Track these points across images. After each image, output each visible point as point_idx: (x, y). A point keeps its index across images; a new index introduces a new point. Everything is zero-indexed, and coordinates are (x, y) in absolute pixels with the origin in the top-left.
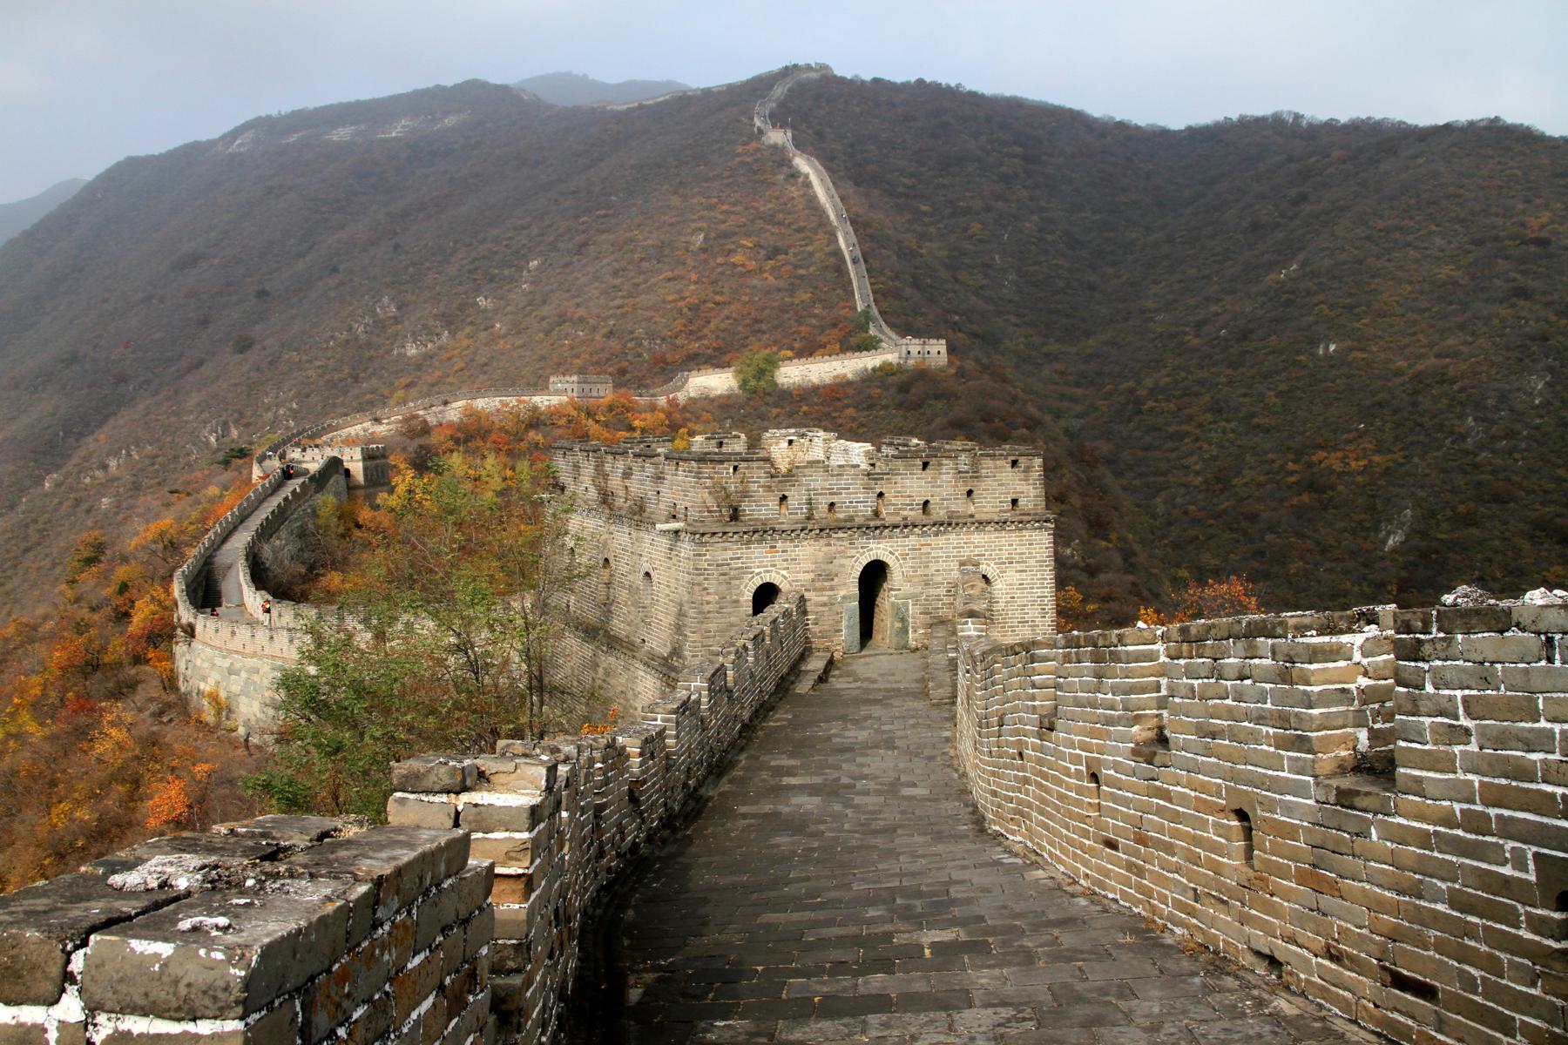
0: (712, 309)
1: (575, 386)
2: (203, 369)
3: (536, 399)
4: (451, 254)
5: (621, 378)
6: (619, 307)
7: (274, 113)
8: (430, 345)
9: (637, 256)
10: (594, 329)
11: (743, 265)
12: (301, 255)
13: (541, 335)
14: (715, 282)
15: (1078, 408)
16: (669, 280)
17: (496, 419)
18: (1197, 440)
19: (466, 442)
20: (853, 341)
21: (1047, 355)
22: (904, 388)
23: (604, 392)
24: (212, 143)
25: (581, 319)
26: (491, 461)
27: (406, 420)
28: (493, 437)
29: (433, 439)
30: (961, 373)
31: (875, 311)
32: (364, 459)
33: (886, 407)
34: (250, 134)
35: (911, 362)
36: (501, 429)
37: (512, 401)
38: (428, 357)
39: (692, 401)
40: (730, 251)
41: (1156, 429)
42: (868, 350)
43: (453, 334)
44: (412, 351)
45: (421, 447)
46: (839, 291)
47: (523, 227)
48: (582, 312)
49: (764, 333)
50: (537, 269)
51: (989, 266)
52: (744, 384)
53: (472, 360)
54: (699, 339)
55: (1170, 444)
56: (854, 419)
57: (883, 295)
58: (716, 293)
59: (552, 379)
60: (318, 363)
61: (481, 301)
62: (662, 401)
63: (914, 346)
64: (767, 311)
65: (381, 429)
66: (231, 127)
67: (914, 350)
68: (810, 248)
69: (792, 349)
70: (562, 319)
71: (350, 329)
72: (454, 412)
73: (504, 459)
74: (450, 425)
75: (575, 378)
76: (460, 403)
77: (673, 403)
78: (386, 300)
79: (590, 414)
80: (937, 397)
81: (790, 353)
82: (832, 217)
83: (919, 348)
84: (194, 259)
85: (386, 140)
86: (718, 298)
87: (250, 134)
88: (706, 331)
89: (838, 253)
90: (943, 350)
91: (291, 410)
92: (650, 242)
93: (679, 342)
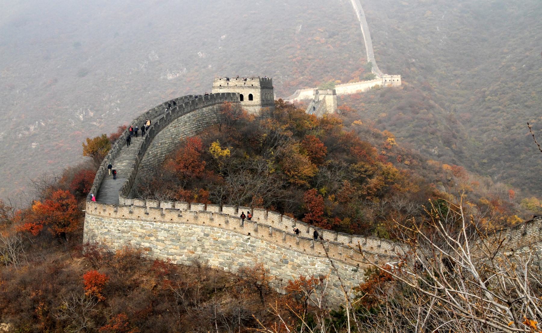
0: (307, 62)
6: (267, 61)
8: (178, 75)
11: (319, 41)
14: (307, 49)
15: (463, 99)
18: (503, 112)
20: (365, 75)
21: (455, 75)
22: (382, 95)
30: (406, 88)
31: (374, 63)
33: (376, 102)
35: (386, 84)
39: (301, 100)
41: (489, 108)
42: (370, 80)
44: (170, 77)
46: (360, 53)
49: (329, 72)
51: (433, 33)
54: (303, 75)
55: (494, 114)
56: (363, 107)
57: (379, 54)
58: (308, 54)
61: (200, 54)
63: (388, 78)
64: (330, 63)
67: (388, 80)
68: (348, 33)
69: (340, 79)
78: (153, 52)
80: (395, 98)
81: (339, 81)
82: (358, 16)
83: (390, 79)
86: (310, 57)
88: (305, 72)
89: (360, 35)
90: (400, 79)
91: (117, 104)
93: (294, 77)
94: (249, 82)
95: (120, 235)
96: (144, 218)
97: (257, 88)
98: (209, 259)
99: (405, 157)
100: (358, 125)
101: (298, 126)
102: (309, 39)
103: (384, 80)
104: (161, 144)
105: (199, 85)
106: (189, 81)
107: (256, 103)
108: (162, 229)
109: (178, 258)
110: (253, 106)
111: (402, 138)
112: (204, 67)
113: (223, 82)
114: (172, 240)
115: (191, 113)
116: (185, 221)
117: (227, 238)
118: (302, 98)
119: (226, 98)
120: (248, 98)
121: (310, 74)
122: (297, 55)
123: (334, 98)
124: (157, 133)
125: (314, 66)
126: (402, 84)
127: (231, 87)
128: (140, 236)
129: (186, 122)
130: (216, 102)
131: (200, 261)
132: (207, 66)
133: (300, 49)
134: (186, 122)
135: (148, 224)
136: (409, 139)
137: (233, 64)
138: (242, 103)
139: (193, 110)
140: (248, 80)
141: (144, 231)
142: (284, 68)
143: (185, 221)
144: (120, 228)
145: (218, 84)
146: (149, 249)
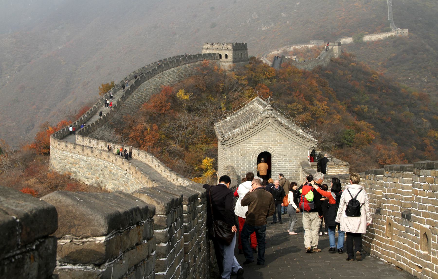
3: (308, 46)
11: (358, 6)
22: (394, 42)
35: (398, 35)
37: (303, 46)
44: (263, 29)
54: (344, 29)
61: (283, 14)
63: (399, 31)
67: (399, 32)
69: (368, 31)
78: (255, 13)
81: (367, 33)
86: (350, 17)
90: (407, 31)
94: (226, 46)
95: (60, 161)
96: (73, 151)
97: (230, 50)
98: (106, 184)
99: (383, 87)
100: (353, 66)
101: (255, 77)
102: (351, 5)
103: (397, 32)
104: (146, 89)
105: (280, 34)
106: (275, 32)
107: (230, 61)
108: (83, 160)
109: (90, 181)
110: (228, 62)
111: (404, 70)
112: (284, 23)
113: (209, 46)
114: (87, 168)
115: (175, 68)
116: (95, 156)
117: (116, 171)
119: (207, 57)
120: (224, 57)
123: (339, 48)
124: (143, 83)
126: (409, 35)
127: (214, 49)
128: (71, 163)
129: (170, 74)
130: (199, 59)
131: (101, 185)
132: (286, 22)
134: (170, 74)
135: (74, 155)
136: (408, 71)
137: (302, 21)
138: (221, 60)
139: (177, 66)
140: (225, 44)
141: (73, 160)
143: (95, 156)
144: (61, 156)
145: (206, 47)
146: (75, 172)
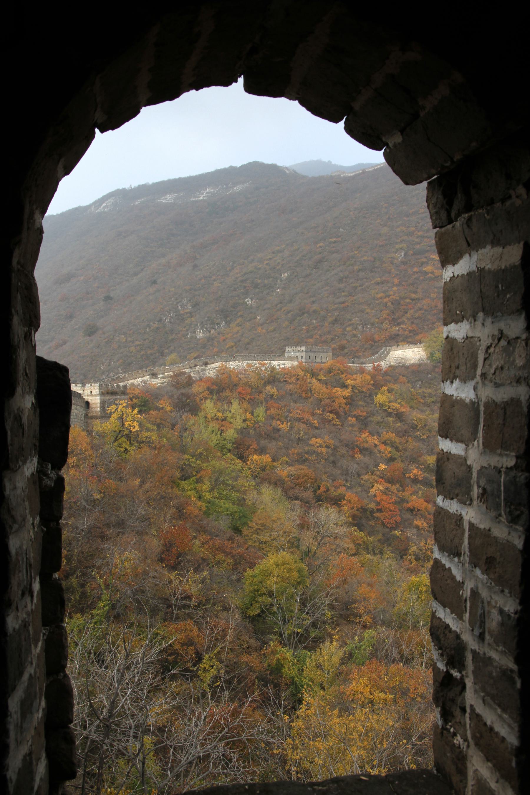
0: (409, 303)
1: (304, 354)
2: (64, 346)
3: (275, 363)
4: (230, 270)
5: (340, 351)
6: (343, 303)
7: (127, 187)
9: (356, 268)
10: (324, 318)
11: (432, 273)
12: (136, 274)
13: (287, 323)
16: (378, 284)
17: (241, 376)
19: (218, 392)
23: (326, 359)
24: (89, 206)
25: (315, 312)
26: (235, 405)
27: (176, 376)
28: (240, 389)
29: (195, 389)
32: (102, 394)
34: (111, 200)
36: (246, 384)
38: (211, 339)
39: (392, 368)
40: (423, 263)
43: (228, 323)
44: (200, 335)
45: (182, 394)
47: (279, 252)
48: (315, 307)
50: (287, 278)
52: (431, 356)
53: (240, 341)
54: (399, 324)
59: (288, 349)
60: (138, 343)
61: (248, 301)
62: (369, 367)
65: (157, 382)
66: (100, 196)
70: (302, 312)
71: (160, 320)
72: (212, 370)
73: (245, 405)
74: (209, 379)
75: (304, 348)
76: (217, 364)
77: (377, 369)
78: (185, 301)
79: (314, 374)
84: (69, 277)
85: (196, 202)
86: (413, 296)
87: (111, 200)
88: (404, 319)
92: (365, 258)
93: (384, 326)
102: (415, 269)
105: (233, 344)
118: (392, 363)
121: (412, 323)
122: (391, 293)
125: (420, 309)
132: (256, 318)
133: (398, 285)
142: (367, 313)
